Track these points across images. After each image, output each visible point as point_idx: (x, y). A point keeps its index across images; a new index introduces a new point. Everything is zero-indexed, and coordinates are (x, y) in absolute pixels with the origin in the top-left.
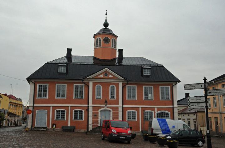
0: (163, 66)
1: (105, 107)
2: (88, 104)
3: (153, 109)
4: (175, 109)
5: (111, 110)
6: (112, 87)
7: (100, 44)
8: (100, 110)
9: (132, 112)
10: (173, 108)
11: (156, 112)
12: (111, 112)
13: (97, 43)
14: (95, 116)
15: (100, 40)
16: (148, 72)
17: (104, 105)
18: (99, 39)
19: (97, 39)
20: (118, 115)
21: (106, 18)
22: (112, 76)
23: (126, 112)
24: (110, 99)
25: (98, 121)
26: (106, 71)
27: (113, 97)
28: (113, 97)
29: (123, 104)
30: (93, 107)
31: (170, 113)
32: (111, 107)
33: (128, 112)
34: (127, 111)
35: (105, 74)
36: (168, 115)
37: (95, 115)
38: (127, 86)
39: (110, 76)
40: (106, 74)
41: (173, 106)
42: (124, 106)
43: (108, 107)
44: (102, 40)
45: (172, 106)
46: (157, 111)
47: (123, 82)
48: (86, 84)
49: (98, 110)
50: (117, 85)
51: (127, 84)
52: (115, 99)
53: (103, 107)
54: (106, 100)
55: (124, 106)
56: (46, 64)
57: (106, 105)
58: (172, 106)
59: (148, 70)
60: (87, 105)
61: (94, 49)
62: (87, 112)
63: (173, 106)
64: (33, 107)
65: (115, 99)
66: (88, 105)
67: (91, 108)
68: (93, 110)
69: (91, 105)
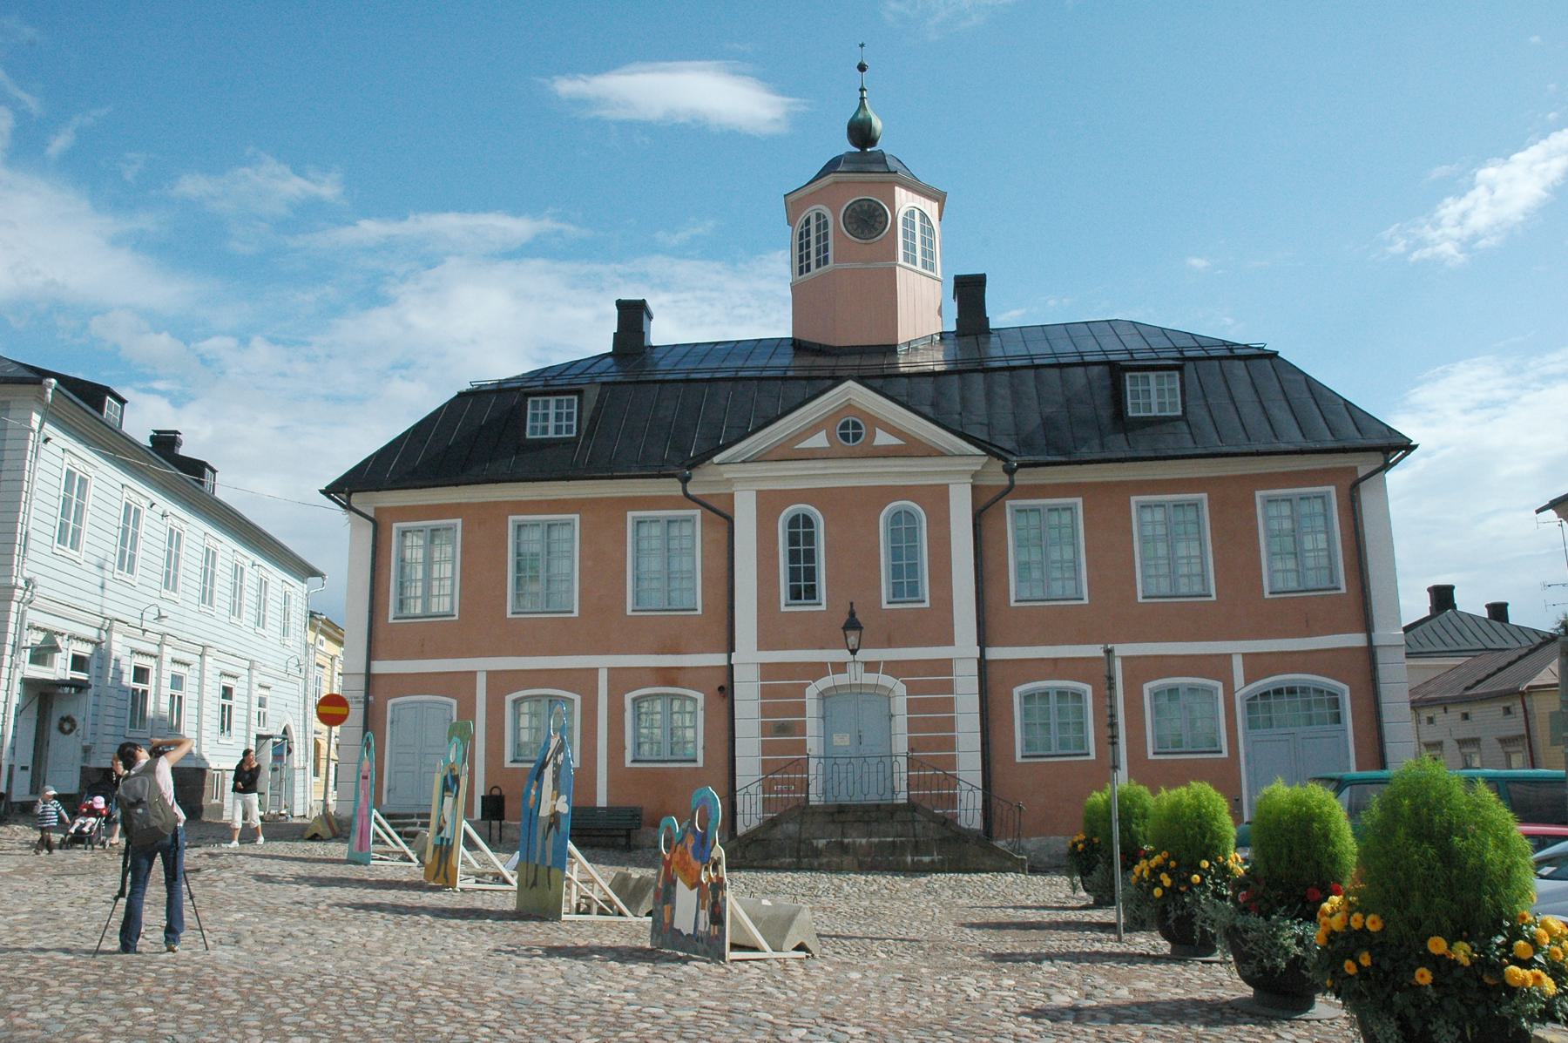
0: (1274, 355)
1: (851, 667)
2: (731, 648)
3: (1218, 667)
4: (1381, 656)
5: (899, 688)
6: (896, 517)
8: (812, 691)
9: (1053, 698)
11: (1242, 689)
12: (900, 704)
13: (804, 246)
14: (782, 730)
15: (822, 224)
16: (1160, 393)
17: (842, 655)
18: (818, 216)
19: (808, 222)
20: (950, 724)
21: (862, 90)
22: (895, 441)
23: (1011, 695)
24: (885, 606)
25: (803, 766)
26: (849, 407)
27: (905, 584)
28: (905, 584)
29: (983, 642)
30: (767, 670)
31: (1346, 688)
32: (893, 668)
33: (1028, 698)
34: (1018, 691)
35: (845, 426)
36: (1335, 702)
37: (783, 729)
38: (1009, 503)
39: (883, 439)
40: (851, 431)
41: (1370, 639)
42: (994, 653)
43: (871, 667)
45: (1357, 640)
46: (1247, 682)
47: (975, 475)
48: (714, 504)
49: (800, 691)
50: (936, 499)
51: (1009, 491)
52: (927, 604)
53: (840, 667)
54: (852, 614)
55: (994, 653)
56: (461, 395)
57: (853, 652)
58: (1357, 640)
59: (1160, 381)
60: (719, 659)
61: (795, 288)
62: (723, 705)
63: (1370, 639)
64: (370, 677)
65: (927, 604)
66: (730, 658)
67: (754, 673)
68: (766, 692)
69: (748, 655)
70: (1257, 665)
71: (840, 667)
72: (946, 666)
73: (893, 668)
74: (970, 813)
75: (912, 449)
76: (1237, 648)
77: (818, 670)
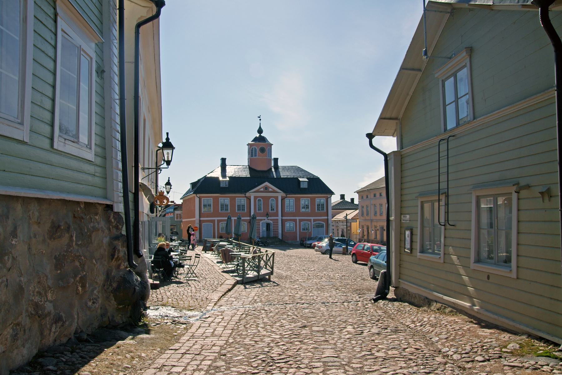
3: (310, 220)
7: (256, 154)
10: (328, 219)
13: (252, 152)
15: (255, 150)
20: (278, 227)
27: (272, 209)
32: (271, 220)
39: (270, 190)
40: (266, 188)
44: (258, 150)
45: (326, 218)
51: (286, 197)
53: (264, 220)
64: (200, 220)
70: (315, 220)
71: (264, 220)
72: (277, 220)
73: (271, 220)
74: (280, 237)
75: (274, 192)
76: (312, 218)
77: (261, 220)
